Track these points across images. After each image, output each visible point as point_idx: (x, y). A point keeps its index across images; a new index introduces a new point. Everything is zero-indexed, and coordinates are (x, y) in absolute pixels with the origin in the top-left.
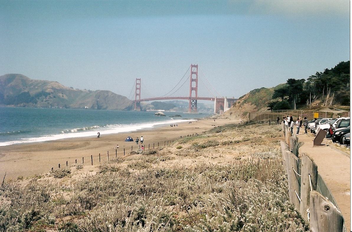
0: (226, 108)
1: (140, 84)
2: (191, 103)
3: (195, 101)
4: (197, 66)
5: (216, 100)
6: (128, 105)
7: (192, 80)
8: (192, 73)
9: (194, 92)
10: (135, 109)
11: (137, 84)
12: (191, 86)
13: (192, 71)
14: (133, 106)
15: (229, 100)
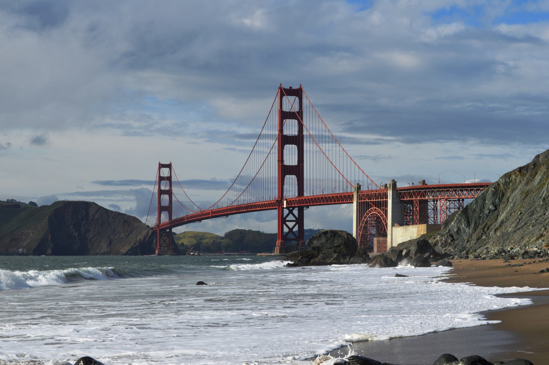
0: (393, 225)
1: (169, 179)
2: (282, 221)
3: (296, 212)
4: (298, 93)
5: (359, 198)
6: (141, 237)
7: (284, 140)
8: (284, 115)
9: (291, 180)
10: (157, 252)
11: (161, 179)
12: (281, 159)
13: (285, 109)
14: (155, 240)
15: (399, 194)
